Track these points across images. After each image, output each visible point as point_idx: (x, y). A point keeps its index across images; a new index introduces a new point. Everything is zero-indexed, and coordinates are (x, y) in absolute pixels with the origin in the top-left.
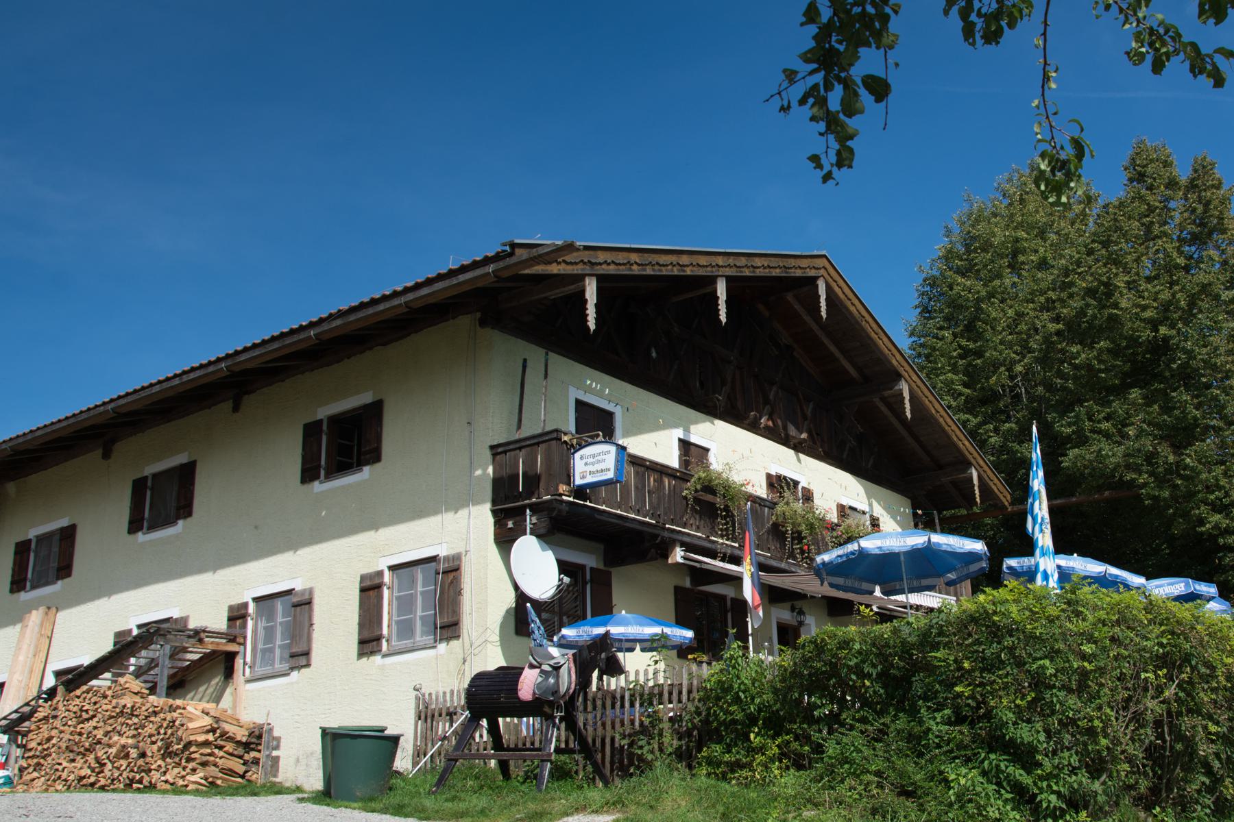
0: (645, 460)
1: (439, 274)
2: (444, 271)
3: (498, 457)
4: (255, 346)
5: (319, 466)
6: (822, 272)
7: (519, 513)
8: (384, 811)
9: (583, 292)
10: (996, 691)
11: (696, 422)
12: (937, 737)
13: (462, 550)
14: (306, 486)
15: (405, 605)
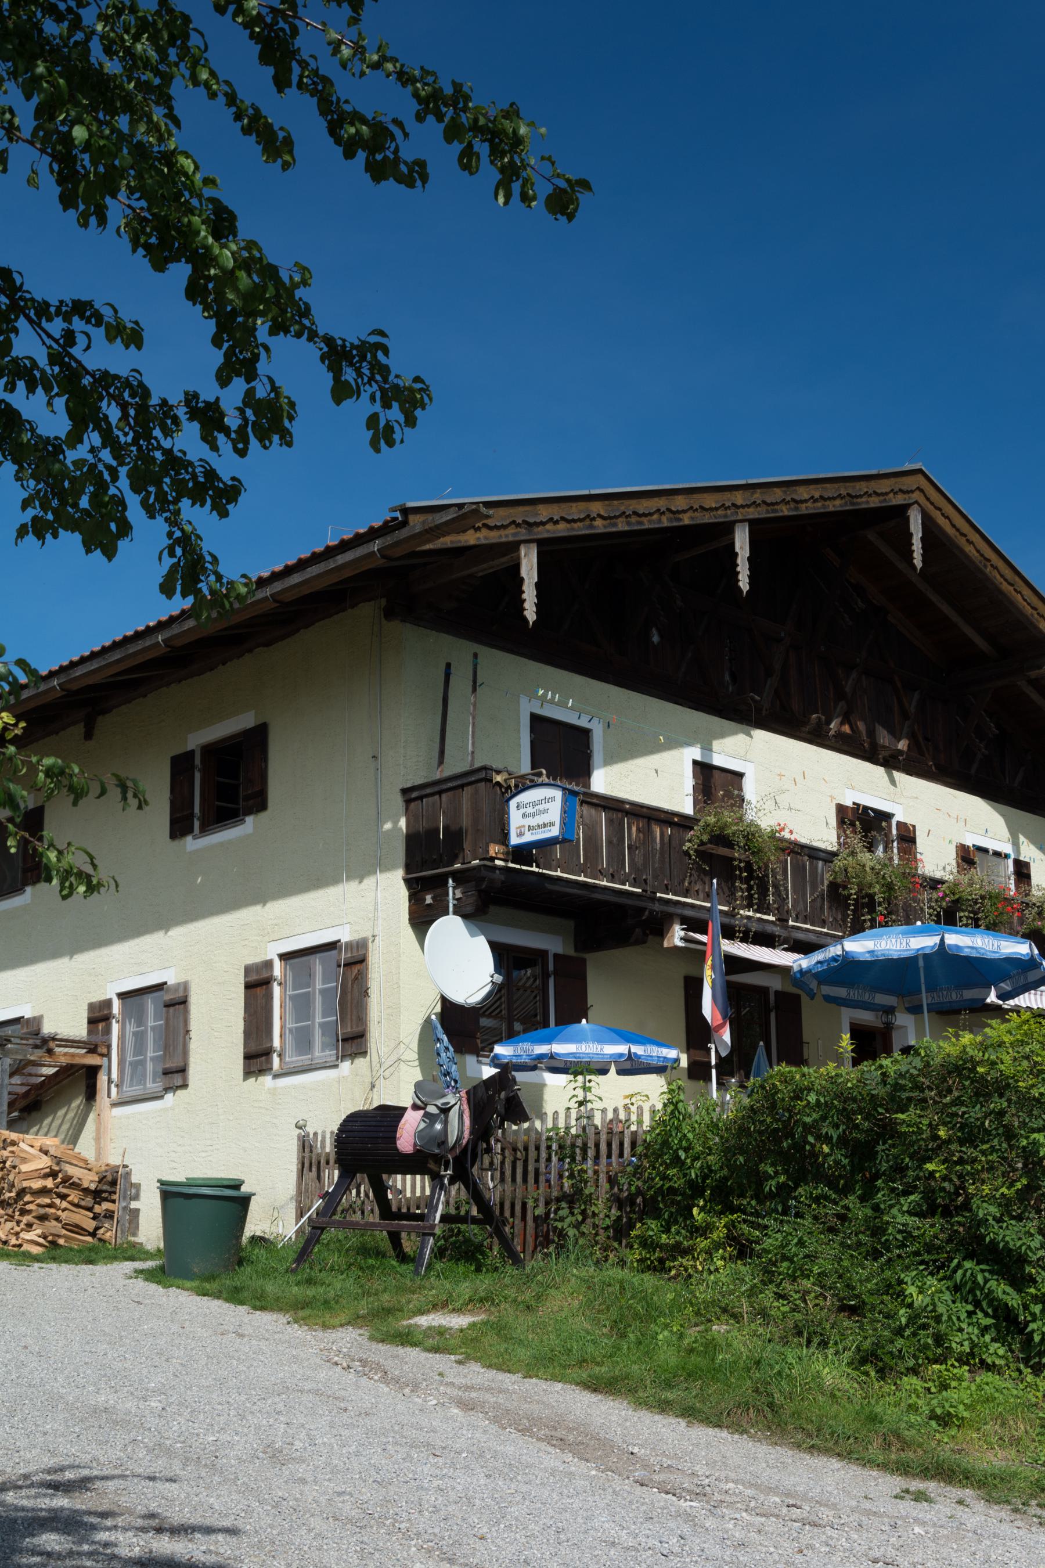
0: (622, 802)
1: (314, 554)
2: (320, 548)
3: (413, 805)
4: (94, 655)
5: (192, 815)
6: (916, 496)
7: (438, 884)
8: (217, 1295)
9: (517, 567)
10: (978, 1172)
11: (722, 735)
12: (900, 1232)
13: (368, 934)
14: (176, 843)
15: (301, 1006)
